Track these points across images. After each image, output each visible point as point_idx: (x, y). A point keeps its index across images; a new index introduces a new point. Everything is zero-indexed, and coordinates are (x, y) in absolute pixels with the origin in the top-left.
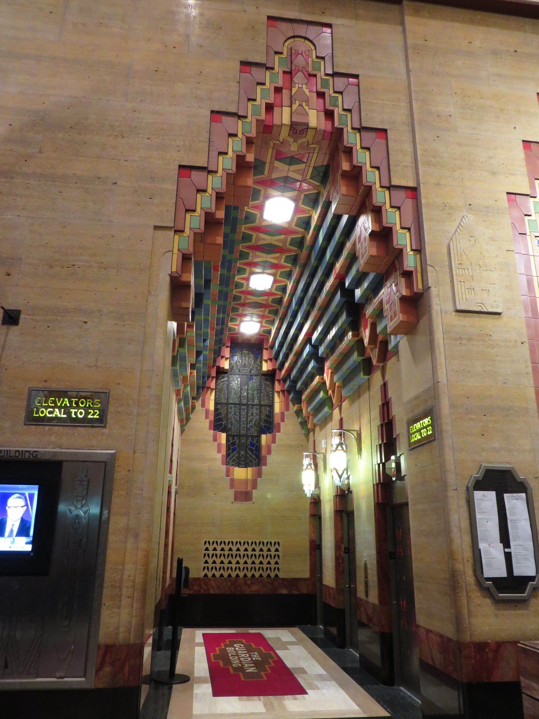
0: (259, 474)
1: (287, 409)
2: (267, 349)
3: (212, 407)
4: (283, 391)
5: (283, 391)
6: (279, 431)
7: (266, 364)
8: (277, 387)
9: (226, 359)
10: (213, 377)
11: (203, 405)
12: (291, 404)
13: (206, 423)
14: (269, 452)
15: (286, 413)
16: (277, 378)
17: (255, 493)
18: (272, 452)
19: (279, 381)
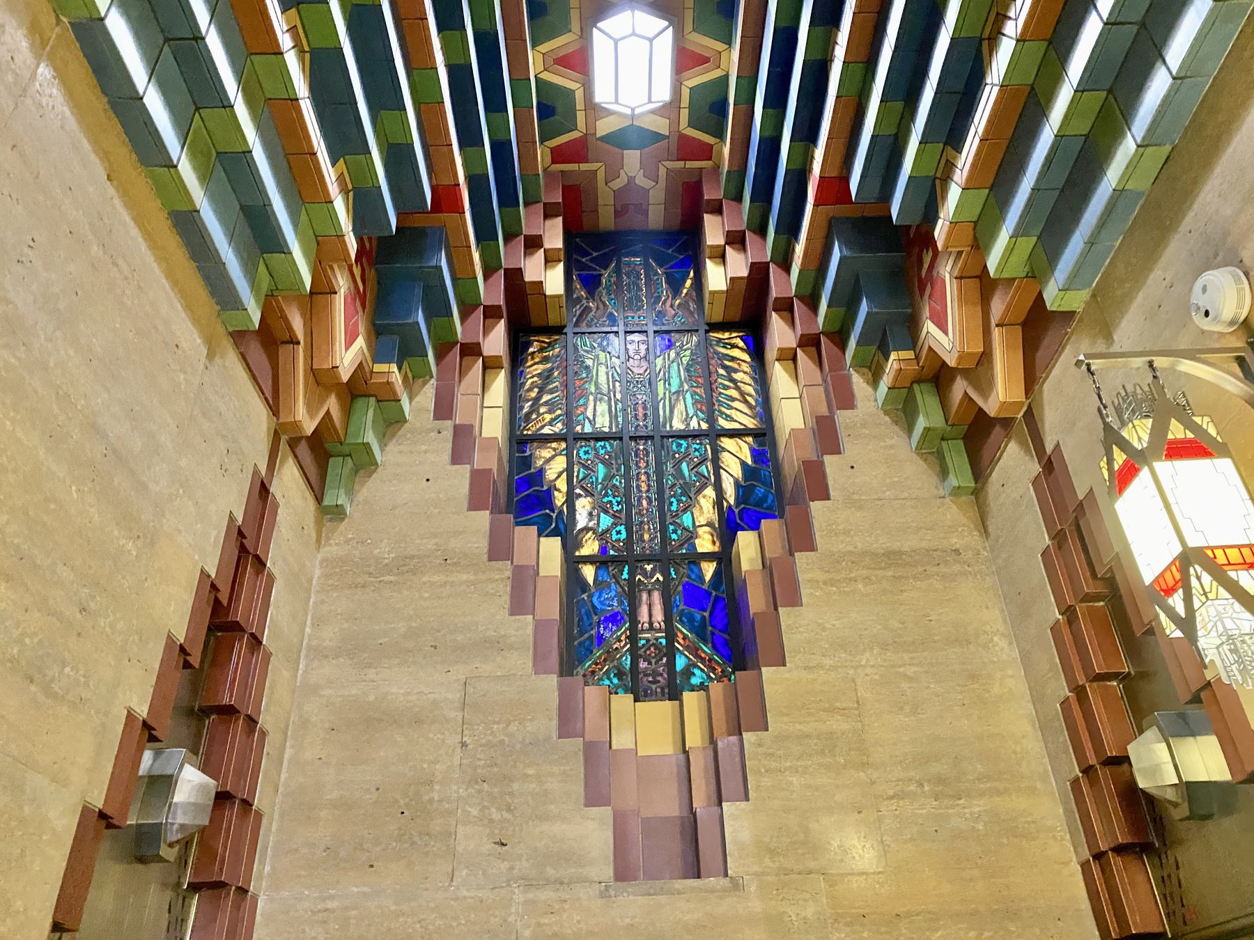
0: (745, 715)
1: (845, 399)
2: (717, 209)
3: (493, 425)
5: (810, 342)
8: (780, 333)
9: (549, 261)
10: (491, 313)
11: (444, 409)
12: (858, 382)
15: (842, 417)
16: (774, 293)
18: (805, 592)
19: (785, 307)
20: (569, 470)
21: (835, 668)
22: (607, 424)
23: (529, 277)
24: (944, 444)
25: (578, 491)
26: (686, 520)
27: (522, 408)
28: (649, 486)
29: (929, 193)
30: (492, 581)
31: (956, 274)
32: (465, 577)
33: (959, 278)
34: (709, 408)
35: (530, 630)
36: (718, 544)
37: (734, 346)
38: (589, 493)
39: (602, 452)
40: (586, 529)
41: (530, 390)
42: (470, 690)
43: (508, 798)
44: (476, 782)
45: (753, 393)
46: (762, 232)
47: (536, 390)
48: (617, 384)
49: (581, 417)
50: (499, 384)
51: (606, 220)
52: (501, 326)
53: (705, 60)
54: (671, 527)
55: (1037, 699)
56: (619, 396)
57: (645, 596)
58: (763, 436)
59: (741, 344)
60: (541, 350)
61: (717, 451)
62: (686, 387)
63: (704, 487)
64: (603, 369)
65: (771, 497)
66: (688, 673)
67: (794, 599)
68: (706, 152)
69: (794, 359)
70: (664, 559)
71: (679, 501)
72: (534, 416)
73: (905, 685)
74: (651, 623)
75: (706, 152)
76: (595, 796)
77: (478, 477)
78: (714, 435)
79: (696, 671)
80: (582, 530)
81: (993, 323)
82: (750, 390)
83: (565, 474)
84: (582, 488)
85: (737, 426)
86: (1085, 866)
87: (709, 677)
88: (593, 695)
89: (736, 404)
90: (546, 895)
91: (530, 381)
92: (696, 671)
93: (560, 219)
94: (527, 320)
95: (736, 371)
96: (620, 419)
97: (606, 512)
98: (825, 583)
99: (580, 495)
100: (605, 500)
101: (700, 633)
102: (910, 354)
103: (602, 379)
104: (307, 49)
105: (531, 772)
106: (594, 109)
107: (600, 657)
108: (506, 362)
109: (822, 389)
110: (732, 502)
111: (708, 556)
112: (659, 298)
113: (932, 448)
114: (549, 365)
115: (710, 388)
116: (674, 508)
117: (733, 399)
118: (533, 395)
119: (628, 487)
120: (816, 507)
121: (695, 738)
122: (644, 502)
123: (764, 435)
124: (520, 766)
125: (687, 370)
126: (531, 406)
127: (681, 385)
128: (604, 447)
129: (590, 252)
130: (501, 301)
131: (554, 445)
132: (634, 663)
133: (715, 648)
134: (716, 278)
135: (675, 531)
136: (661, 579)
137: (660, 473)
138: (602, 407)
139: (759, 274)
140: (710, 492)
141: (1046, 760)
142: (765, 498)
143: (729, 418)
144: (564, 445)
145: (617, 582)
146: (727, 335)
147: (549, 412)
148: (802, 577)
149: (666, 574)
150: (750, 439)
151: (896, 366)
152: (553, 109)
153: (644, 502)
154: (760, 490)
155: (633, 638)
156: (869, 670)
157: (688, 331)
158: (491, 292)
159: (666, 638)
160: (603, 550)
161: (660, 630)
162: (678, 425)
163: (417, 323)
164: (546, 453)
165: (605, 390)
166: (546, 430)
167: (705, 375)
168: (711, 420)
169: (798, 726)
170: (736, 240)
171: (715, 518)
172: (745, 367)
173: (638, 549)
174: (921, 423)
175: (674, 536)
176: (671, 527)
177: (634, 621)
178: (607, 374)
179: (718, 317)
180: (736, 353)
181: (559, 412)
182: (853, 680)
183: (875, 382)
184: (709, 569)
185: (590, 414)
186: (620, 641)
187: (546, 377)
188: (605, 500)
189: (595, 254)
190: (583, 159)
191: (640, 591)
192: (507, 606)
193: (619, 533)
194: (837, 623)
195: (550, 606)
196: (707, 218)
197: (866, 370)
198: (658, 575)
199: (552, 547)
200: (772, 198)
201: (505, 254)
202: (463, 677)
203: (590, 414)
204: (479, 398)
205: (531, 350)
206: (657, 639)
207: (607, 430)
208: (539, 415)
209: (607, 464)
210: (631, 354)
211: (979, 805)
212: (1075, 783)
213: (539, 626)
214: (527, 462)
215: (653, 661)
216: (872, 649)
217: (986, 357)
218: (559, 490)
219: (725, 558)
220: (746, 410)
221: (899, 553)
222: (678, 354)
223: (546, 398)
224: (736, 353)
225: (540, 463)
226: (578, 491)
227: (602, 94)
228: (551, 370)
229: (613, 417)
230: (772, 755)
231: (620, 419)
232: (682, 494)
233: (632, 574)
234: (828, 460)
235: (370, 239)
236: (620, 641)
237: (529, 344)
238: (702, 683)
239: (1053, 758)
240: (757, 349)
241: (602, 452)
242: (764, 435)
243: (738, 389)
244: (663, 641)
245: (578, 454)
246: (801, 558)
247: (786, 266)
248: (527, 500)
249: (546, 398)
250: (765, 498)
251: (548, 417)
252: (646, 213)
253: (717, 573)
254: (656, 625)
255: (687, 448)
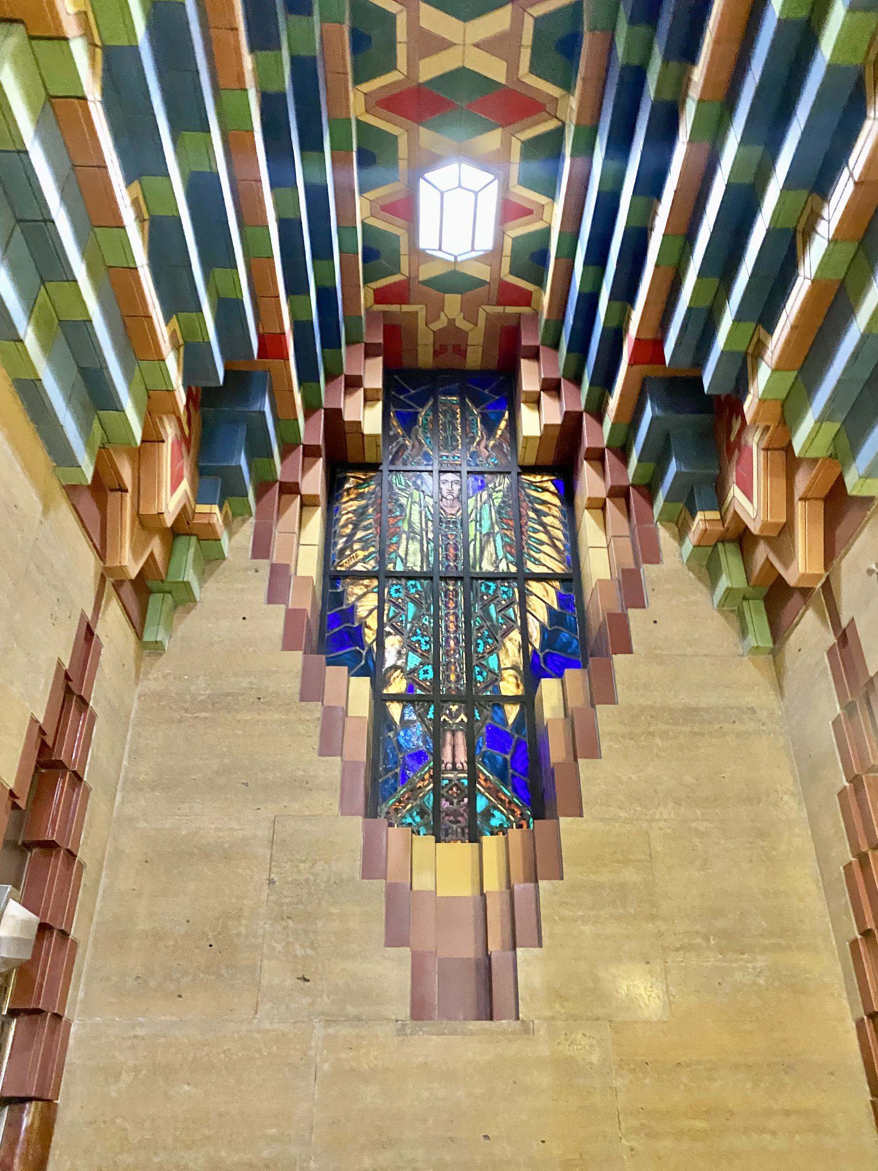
0: (542, 863)
2: (534, 355)
3: (308, 565)
4: (620, 493)
5: (620, 493)
6: (627, 648)
7: (536, 414)
8: (590, 482)
10: (311, 452)
11: (261, 547)
12: (665, 536)
13: (274, 620)
14: (584, 743)
15: (648, 571)
16: (587, 442)
17: (532, 967)
18: (604, 745)
19: (597, 457)
20: (380, 608)
21: (629, 821)
22: (419, 564)
23: (348, 417)
24: (745, 603)
25: (388, 629)
26: (492, 662)
27: (336, 544)
28: (457, 627)
29: (741, 367)
30: (301, 721)
31: (763, 444)
32: (276, 716)
33: (766, 449)
34: (519, 550)
35: (337, 772)
36: (521, 687)
37: (545, 490)
38: (399, 632)
39: (413, 591)
40: (395, 667)
41: (345, 526)
42: (278, 827)
43: (312, 936)
44: (283, 919)
45: (562, 537)
46: (577, 381)
47: (351, 526)
48: (430, 524)
49: (393, 556)
50: (316, 520)
51: (425, 358)
52: (320, 463)
53: (529, 212)
54: (477, 669)
55: (822, 859)
56: (431, 536)
57: (449, 736)
58: (570, 581)
59: (552, 488)
60: (358, 486)
61: (524, 595)
62: (497, 529)
63: (510, 629)
64: (416, 508)
65: (575, 643)
66: (488, 814)
67: (594, 752)
68: (525, 298)
69: (603, 508)
70: (469, 700)
71: (485, 643)
72: (348, 552)
73: (696, 841)
74: (454, 764)
75: (525, 298)
76: (395, 936)
77: (292, 616)
78: (523, 578)
79: (496, 813)
80: (391, 668)
81: (797, 498)
82: (559, 534)
83: (375, 612)
84: (393, 626)
85: (544, 570)
86: (860, 1024)
87: (508, 819)
88: (396, 835)
89: (545, 548)
90: (344, 1031)
91: (344, 518)
92: (496, 813)
93: (380, 359)
94: (345, 458)
95: (546, 515)
96: (431, 559)
97: (414, 651)
98: (623, 736)
99: (389, 634)
100: (414, 639)
101: (502, 776)
102: (715, 515)
103: (415, 518)
104: (146, 217)
105: (334, 911)
106: (419, 256)
107: (403, 795)
108: (322, 500)
109: (628, 540)
110: (537, 645)
111: (513, 700)
112: (474, 438)
113: (733, 607)
114: (363, 502)
115: (520, 531)
116: (480, 649)
117: (542, 543)
118: (348, 531)
119: (437, 626)
120: (619, 660)
121: (493, 883)
122: (452, 643)
123: (571, 580)
124: (324, 904)
125: (499, 512)
126: (346, 542)
127: (492, 526)
128: (414, 586)
129: (409, 389)
130: (321, 442)
131: (366, 582)
132: (437, 802)
133: (515, 790)
134: (531, 423)
135: (480, 673)
136: (465, 720)
137: (468, 615)
138: (414, 546)
139: (573, 422)
140: (516, 635)
141: (828, 919)
142: (570, 643)
143: (537, 562)
144: (375, 583)
145: (423, 722)
146: (538, 478)
147: (363, 549)
148: (602, 729)
149: (470, 715)
150: (557, 584)
151: (702, 526)
152: (376, 254)
153: (452, 643)
154: (565, 636)
155: (436, 778)
156: (662, 824)
157: (501, 473)
158: (310, 431)
159: (468, 779)
160: (410, 688)
161: (462, 771)
162: (487, 566)
163: (240, 466)
164: (358, 590)
165: (418, 529)
166: (359, 567)
167: (515, 517)
168: (520, 564)
169: (593, 877)
170: (552, 387)
171: (519, 659)
172: (555, 511)
173: (444, 690)
174: (724, 583)
175: (479, 678)
176: (477, 669)
177: (438, 760)
178: (420, 513)
179: (531, 460)
180: (546, 496)
181: (372, 549)
182: (647, 833)
183: (681, 535)
184: (512, 712)
185: (402, 552)
186: (423, 780)
187: (361, 513)
188: (414, 639)
189: (413, 392)
190: (404, 301)
191: (445, 731)
192: (317, 747)
193: (426, 672)
194: (634, 777)
195: (358, 747)
196: (524, 364)
197: (673, 525)
198: (463, 717)
199: (361, 686)
200: (590, 354)
201: (326, 392)
202: (271, 816)
203: (402, 552)
204: (296, 536)
205: (347, 486)
206: (459, 779)
207: (418, 569)
208: (353, 551)
209: (417, 603)
210: (445, 493)
211: (761, 962)
212: (854, 944)
213: (347, 768)
214: (339, 598)
215: (455, 801)
216: (665, 806)
217: (787, 529)
218: (369, 627)
219: (528, 701)
220: (555, 555)
221: (696, 710)
222: (490, 496)
223: (360, 534)
224: (546, 496)
225: (352, 599)
226: (388, 629)
227: (427, 241)
228: (366, 507)
229: (424, 556)
230: (567, 903)
231: (431, 559)
232: (489, 637)
233: (437, 714)
234: (631, 612)
235: (197, 387)
236: (423, 780)
237: (345, 479)
238: (501, 825)
239: (835, 919)
240: (567, 492)
241: (413, 591)
242: (571, 580)
243: (547, 532)
244: (466, 782)
245: (389, 592)
246: (603, 711)
247: (599, 417)
248: (337, 637)
249: (360, 534)
250: (570, 643)
251: (361, 554)
252: (464, 354)
253: (520, 716)
254: (459, 766)
255: (495, 591)
